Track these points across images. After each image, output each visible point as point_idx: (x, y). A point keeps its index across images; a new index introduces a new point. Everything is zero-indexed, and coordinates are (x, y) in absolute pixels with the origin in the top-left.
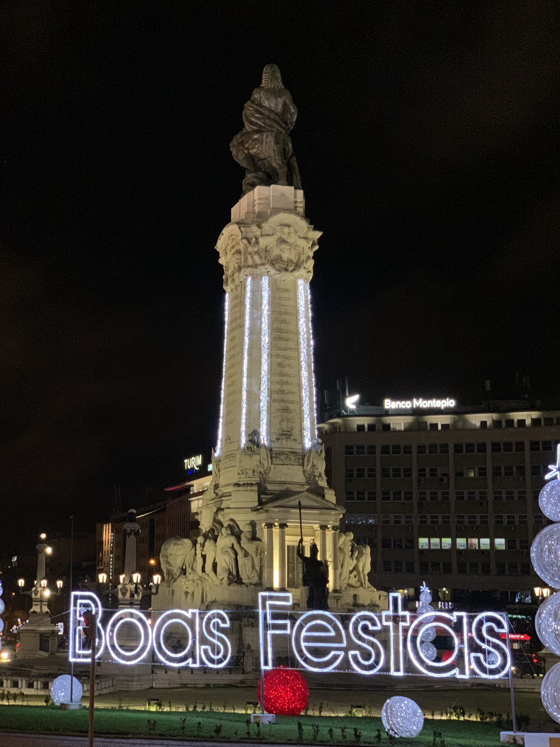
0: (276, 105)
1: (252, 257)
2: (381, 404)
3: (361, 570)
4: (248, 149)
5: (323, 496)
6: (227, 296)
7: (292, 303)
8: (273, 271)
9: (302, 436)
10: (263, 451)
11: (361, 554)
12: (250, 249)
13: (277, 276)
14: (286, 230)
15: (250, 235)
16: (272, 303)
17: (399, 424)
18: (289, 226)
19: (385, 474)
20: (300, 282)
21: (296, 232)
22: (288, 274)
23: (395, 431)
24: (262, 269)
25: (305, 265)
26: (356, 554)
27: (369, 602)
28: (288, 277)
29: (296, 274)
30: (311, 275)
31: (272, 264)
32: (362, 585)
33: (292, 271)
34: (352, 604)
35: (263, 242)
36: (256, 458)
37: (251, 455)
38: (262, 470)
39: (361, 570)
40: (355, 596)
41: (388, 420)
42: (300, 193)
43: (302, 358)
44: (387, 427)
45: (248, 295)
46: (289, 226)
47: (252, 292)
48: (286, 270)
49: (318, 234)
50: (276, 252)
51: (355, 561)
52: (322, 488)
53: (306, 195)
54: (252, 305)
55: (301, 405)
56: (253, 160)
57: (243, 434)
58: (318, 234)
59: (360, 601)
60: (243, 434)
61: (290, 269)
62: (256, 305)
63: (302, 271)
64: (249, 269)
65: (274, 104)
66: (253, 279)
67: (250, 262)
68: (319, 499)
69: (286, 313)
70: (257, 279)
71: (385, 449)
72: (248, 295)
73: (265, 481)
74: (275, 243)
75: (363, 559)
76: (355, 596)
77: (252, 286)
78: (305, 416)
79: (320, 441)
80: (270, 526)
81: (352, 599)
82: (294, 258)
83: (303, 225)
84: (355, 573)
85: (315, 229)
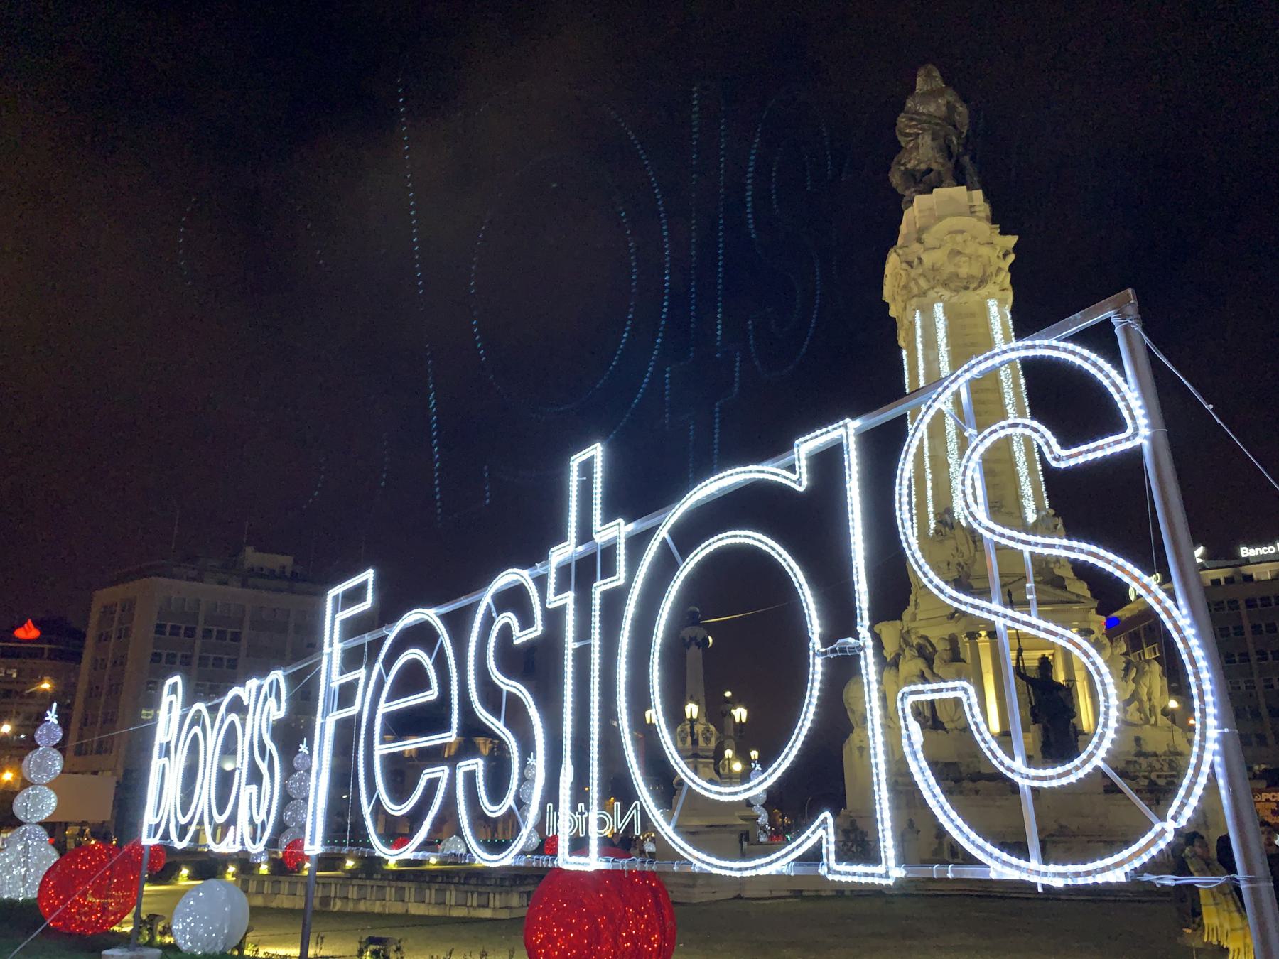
0: (938, 107)
1: (917, 283)
2: (1238, 557)
3: (1145, 698)
4: (904, 164)
5: (1065, 588)
6: (904, 353)
7: (981, 330)
8: (946, 294)
9: (1021, 508)
10: (958, 532)
11: (1141, 673)
12: (913, 273)
13: (954, 299)
14: (959, 238)
15: (910, 258)
16: (950, 335)
17: (1263, 572)
18: (962, 232)
19: (1256, 629)
20: (993, 306)
21: (974, 238)
22: (969, 293)
23: (1259, 581)
24: (932, 294)
25: (994, 279)
26: (1133, 673)
27: (1166, 748)
28: (972, 297)
29: (983, 291)
30: (1010, 296)
31: (945, 285)
32: (1147, 721)
33: (975, 289)
34: (1133, 752)
35: (928, 259)
36: (950, 544)
37: (941, 542)
38: (961, 560)
39: (1145, 698)
40: (1138, 740)
41: (1247, 570)
42: (978, 195)
43: (1007, 401)
44: (1249, 578)
45: (919, 332)
46: (962, 232)
47: (923, 327)
48: (967, 288)
49: (1012, 240)
50: (949, 269)
51: (1132, 686)
52: (1062, 579)
53: (988, 196)
54: (925, 345)
55: (1013, 464)
56: (913, 176)
57: (931, 516)
58: (1012, 240)
59: (1149, 748)
60: (931, 516)
61: (972, 286)
62: (930, 343)
63: (990, 288)
64: (915, 299)
65: (935, 107)
66: (923, 312)
67: (915, 290)
68: (1059, 592)
69: (973, 344)
70: (927, 312)
71: (1250, 603)
72: (919, 332)
73: (968, 576)
74: (945, 258)
75: (1146, 680)
76: (1138, 740)
77: (923, 321)
78: (1023, 479)
79: (1052, 512)
80: (973, 636)
81: (1134, 744)
82: (976, 271)
83: (985, 229)
84: (1136, 704)
85: (1004, 232)
